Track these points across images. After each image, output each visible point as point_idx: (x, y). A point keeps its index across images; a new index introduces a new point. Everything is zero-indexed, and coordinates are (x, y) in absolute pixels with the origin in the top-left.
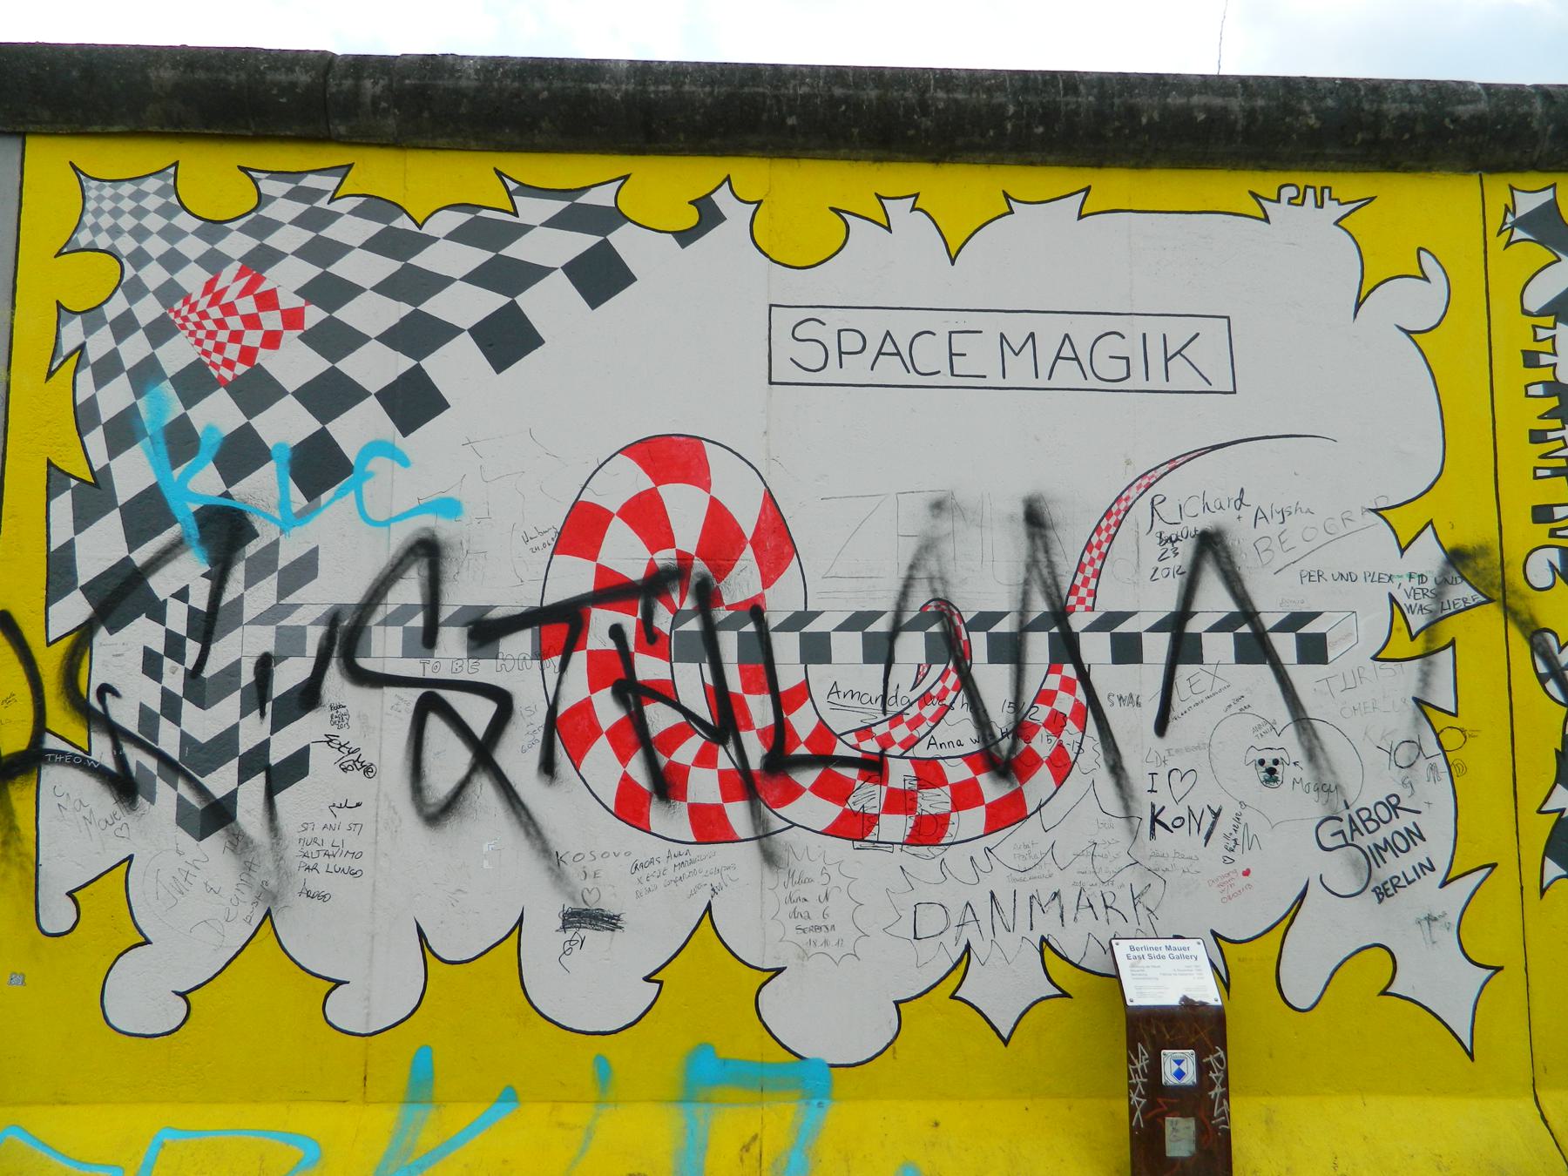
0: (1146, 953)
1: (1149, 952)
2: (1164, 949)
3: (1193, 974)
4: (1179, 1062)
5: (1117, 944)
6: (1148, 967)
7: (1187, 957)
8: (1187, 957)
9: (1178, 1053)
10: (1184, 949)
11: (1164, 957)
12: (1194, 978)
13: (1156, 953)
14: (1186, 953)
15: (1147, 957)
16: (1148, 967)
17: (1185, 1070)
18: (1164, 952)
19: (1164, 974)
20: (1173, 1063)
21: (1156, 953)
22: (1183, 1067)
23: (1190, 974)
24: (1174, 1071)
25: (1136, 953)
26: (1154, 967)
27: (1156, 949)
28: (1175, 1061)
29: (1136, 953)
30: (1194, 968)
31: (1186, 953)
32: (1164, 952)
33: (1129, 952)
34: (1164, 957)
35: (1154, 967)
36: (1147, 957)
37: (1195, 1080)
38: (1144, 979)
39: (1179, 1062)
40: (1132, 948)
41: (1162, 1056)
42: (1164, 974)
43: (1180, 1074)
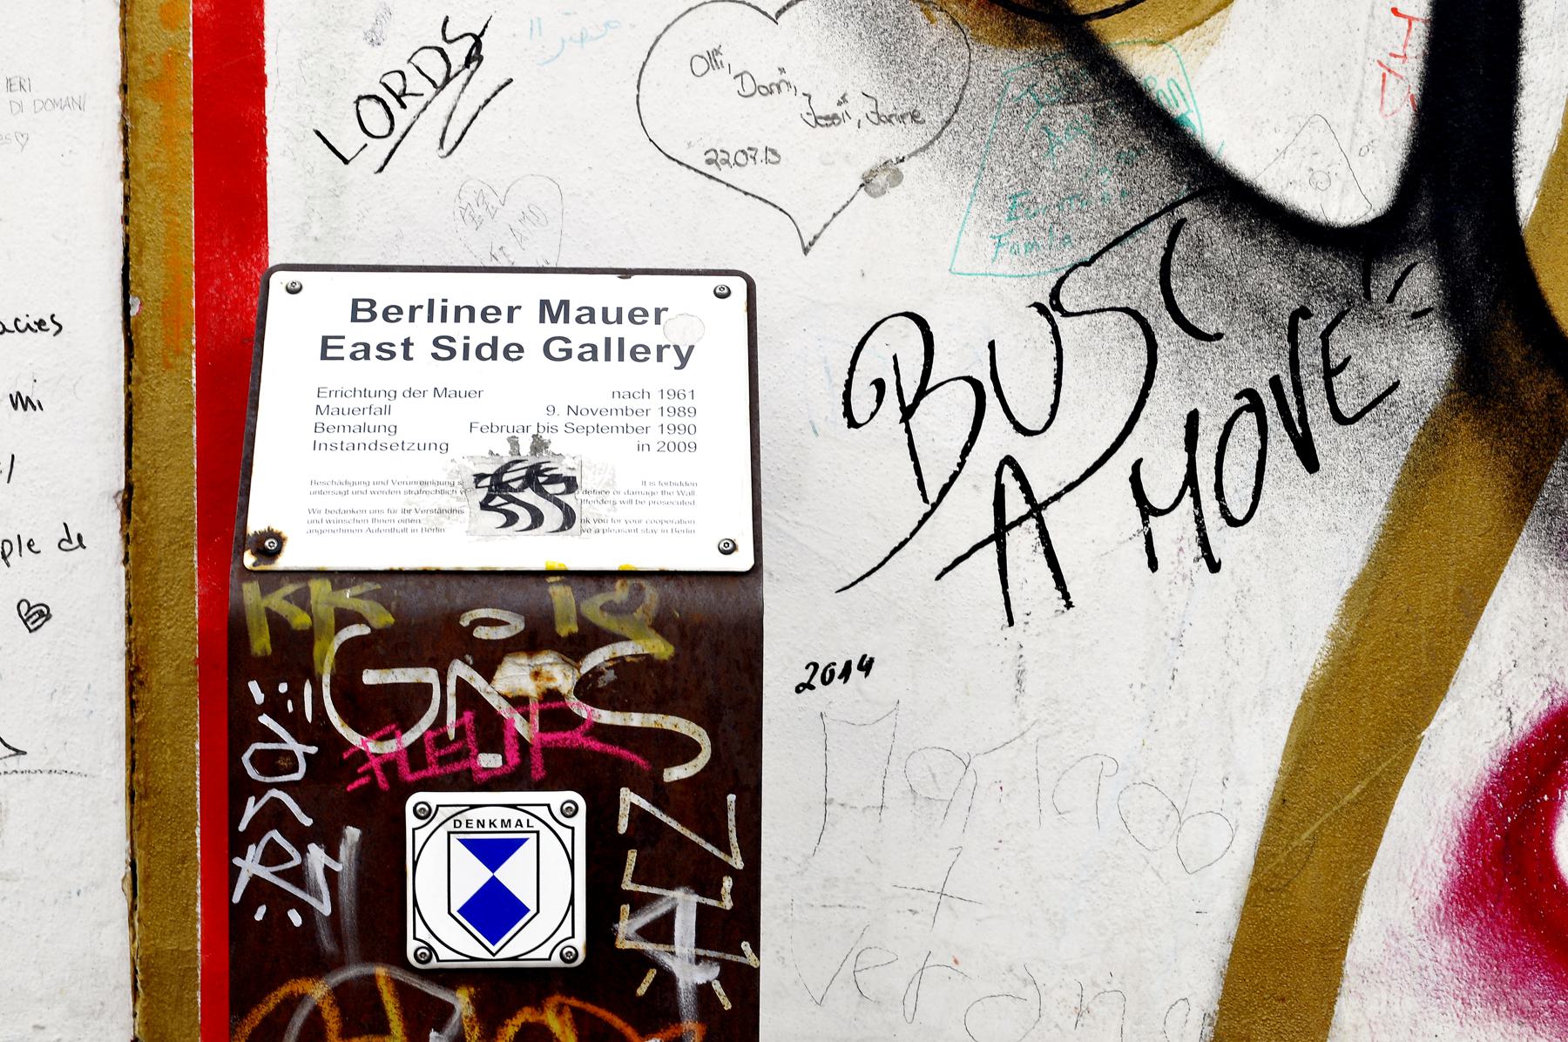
0: (423, 333)
1: (450, 328)
4: (493, 852)
8: (638, 353)
11: (514, 352)
12: (640, 448)
13: (480, 332)
14: (633, 335)
15: (422, 349)
17: (526, 896)
18: (529, 331)
20: (462, 855)
21: (480, 332)
22: (515, 875)
23: (625, 429)
24: (461, 898)
25: (376, 332)
27: (488, 314)
28: (473, 846)
29: (376, 332)
30: (655, 403)
31: (633, 335)
33: (338, 322)
34: (514, 352)
36: (422, 349)
37: (579, 942)
39: (493, 852)
40: (361, 310)
41: (411, 821)
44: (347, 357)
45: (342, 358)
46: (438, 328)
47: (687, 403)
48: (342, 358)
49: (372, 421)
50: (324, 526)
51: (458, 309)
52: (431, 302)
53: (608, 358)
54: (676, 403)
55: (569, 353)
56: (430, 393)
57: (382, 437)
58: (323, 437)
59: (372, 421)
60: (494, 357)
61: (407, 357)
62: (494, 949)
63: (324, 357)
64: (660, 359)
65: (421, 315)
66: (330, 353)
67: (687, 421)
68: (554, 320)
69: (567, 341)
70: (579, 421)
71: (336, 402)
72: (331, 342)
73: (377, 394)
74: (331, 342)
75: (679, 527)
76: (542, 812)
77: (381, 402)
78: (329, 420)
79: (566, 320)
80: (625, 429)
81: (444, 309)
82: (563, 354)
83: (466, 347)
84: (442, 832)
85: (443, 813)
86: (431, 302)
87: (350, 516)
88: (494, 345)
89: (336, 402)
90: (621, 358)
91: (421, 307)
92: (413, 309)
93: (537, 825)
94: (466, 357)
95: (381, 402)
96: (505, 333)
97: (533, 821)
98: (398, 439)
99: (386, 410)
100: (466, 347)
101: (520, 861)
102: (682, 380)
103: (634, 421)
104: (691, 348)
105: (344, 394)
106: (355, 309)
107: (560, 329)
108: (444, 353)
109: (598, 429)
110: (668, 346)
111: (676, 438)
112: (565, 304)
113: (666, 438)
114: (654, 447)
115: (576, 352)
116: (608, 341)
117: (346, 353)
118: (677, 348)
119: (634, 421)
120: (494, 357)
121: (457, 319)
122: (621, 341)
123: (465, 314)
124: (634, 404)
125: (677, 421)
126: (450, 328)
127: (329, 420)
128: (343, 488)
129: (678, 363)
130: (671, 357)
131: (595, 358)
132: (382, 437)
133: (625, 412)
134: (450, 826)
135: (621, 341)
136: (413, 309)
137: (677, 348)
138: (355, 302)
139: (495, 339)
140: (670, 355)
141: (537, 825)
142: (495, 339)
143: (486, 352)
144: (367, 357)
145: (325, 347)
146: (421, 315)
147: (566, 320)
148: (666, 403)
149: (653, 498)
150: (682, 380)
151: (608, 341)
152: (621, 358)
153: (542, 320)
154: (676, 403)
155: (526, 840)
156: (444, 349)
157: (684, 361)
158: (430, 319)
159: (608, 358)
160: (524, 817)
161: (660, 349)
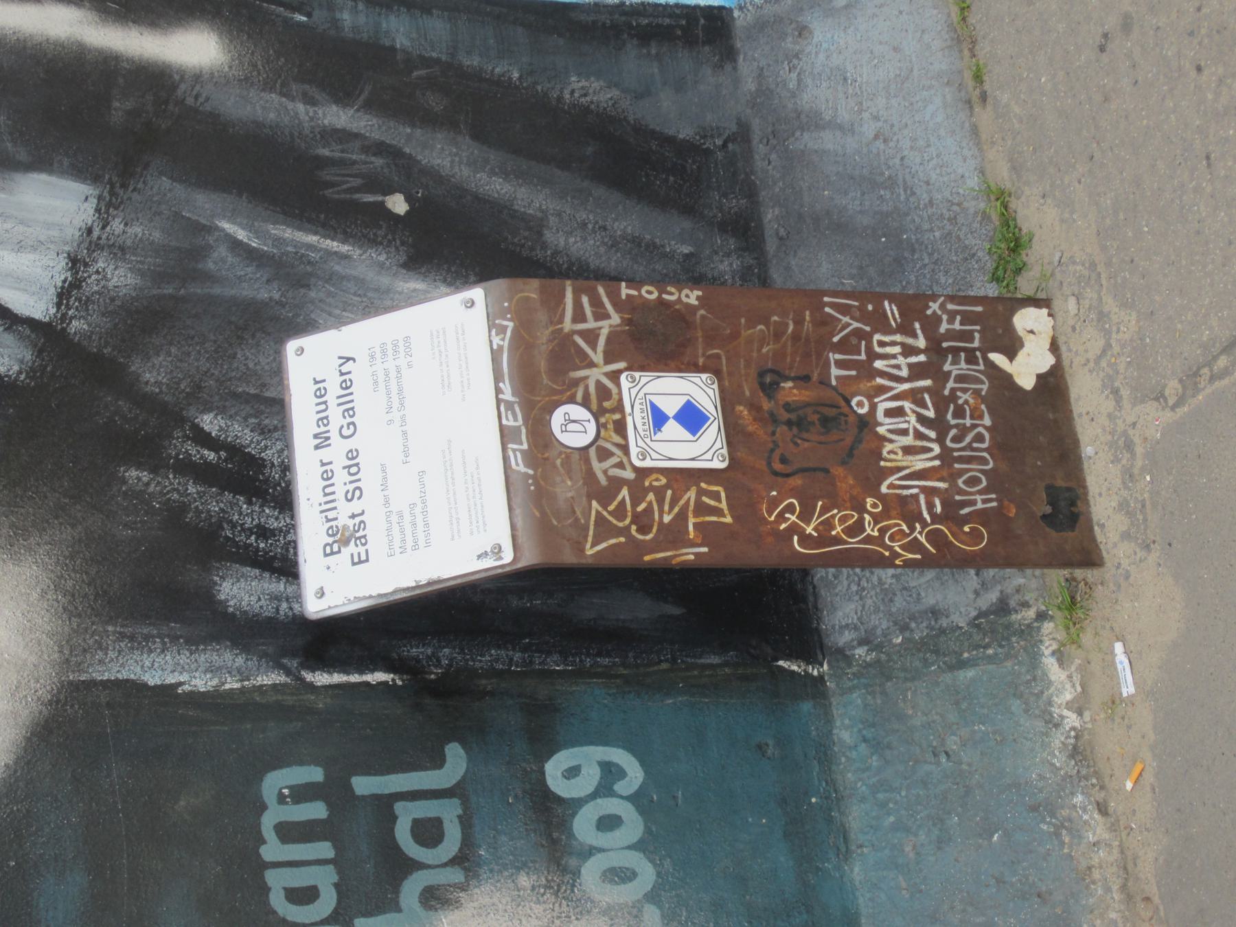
1: (340, 496)
2: (324, 454)
3: (398, 368)
4: (659, 418)
5: (321, 593)
6: (387, 502)
7: (346, 386)
8: (346, 386)
9: (637, 420)
10: (320, 394)
11: (352, 455)
12: (410, 366)
13: (341, 477)
14: (334, 390)
16: (387, 502)
18: (336, 452)
19: (406, 453)
21: (341, 477)
22: (671, 407)
23: (399, 378)
26: (384, 487)
27: (327, 477)
32: (336, 452)
34: (352, 455)
35: (384, 487)
36: (356, 506)
38: (425, 512)
42: (406, 453)
43: (691, 418)
44: (366, 547)
45: (367, 551)
46: (341, 503)
47: (378, 350)
48: (367, 551)
49: (407, 518)
50: (481, 522)
51: (326, 495)
52: (322, 512)
53: (352, 401)
54: (378, 355)
55: (349, 424)
56: (386, 493)
57: (418, 510)
58: (421, 543)
59: (407, 518)
60: (357, 465)
61: (363, 513)
62: (712, 418)
63: (367, 560)
64: (350, 373)
65: (331, 515)
66: (363, 557)
67: (389, 347)
68: (328, 438)
69: (342, 427)
70: (396, 404)
71: (397, 543)
72: (356, 560)
73: (389, 522)
74: (356, 560)
75: (460, 332)
76: (634, 392)
77: (394, 518)
78: (410, 543)
79: (328, 431)
80: (399, 378)
81: (326, 503)
82: (351, 426)
83: (351, 482)
84: (652, 444)
85: (641, 443)
86: (322, 512)
87: (473, 512)
88: (349, 467)
89: (397, 543)
90: (351, 394)
91: (326, 517)
92: (328, 520)
93: (641, 395)
94: (359, 480)
95: (394, 518)
96: (340, 461)
97: (639, 396)
98: (419, 502)
99: (401, 516)
100: (351, 482)
101: (662, 404)
102: (363, 359)
103: (393, 374)
104: (340, 358)
105: (391, 541)
106: (332, 553)
107: (334, 434)
108: (357, 493)
109: (400, 391)
110: (340, 371)
111: (402, 349)
112: (316, 436)
113: (402, 354)
114: (409, 359)
115: (349, 420)
116: (339, 405)
117: (362, 550)
118: (340, 366)
119: (393, 374)
120: (357, 465)
121: (333, 493)
122: (339, 397)
123: (328, 490)
124: (381, 378)
125: (390, 352)
126: (340, 496)
127: (410, 543)
128: (454, 521)
129: (351, 362)
131: (352, 409)
132: (418, 510)
133: (387, 381)
134: (648, 440)
135: (339, 397)
136: (328, 520)
137: (340, 366)
138: (326, 555)
139: (344, 468)
140: (344, 369)
141: (641, 395)
142: (344, 468)
143: (354, 470)
144: (364, 537)
145: (360, 562)
146: (331, 515)
147: (328, 431)
148: (379, 361)
149: (443, 350)
150: (363, 359)
151: (339, 405)
153: (329, 445)
154: (378, 355)
155: (651, 402)
156: (354, 494)
157: (348, 359)
158: (335, 508)
160: (637, 402)
161: (342, 374)
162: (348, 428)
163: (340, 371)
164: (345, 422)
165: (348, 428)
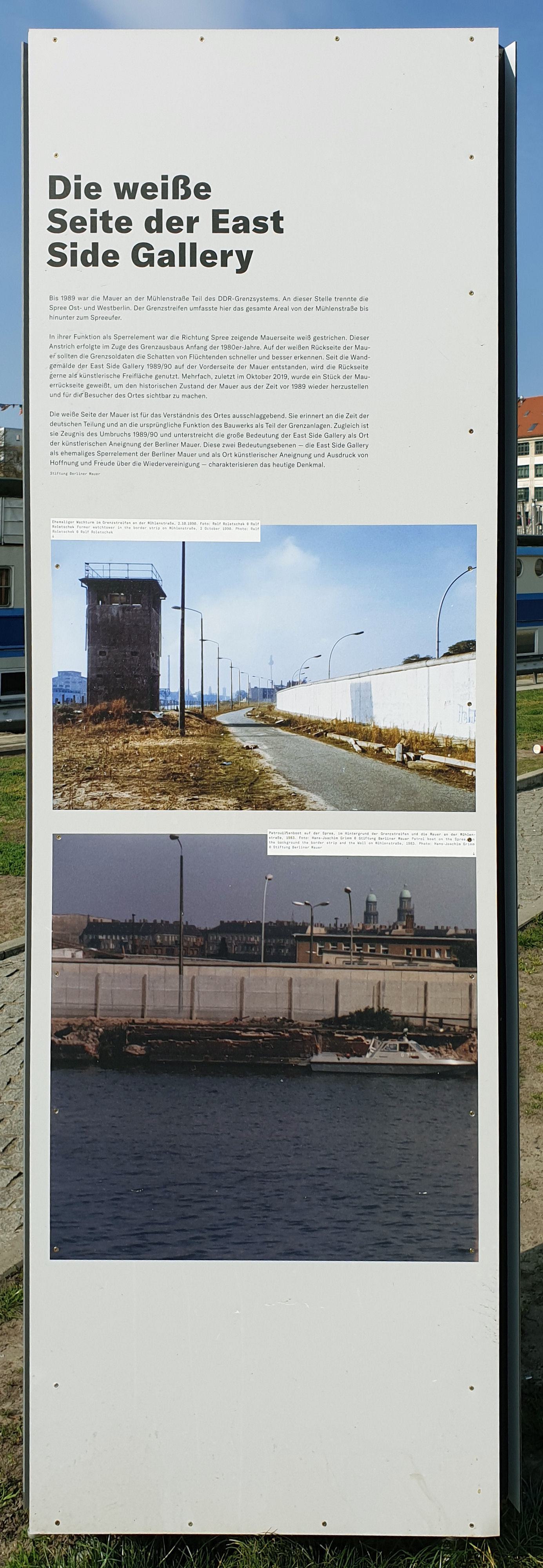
53: (182, 264)
55: (151, 257)
69: (150, 247)
82: (146, 260)
83: (74, 253)
90: (193, 264)
104: (250, 253)
110: (231, 253)
115: (157, 258)
118: (239, 253)
120: (95, 263)
122: (193, 246)
129: (239, 267)
130: (234, 262)
131: (172, 264)
137: (239, 253)
143: (90, 258)
152: (193, 264)
159: (182, 264)
162: (145, 255)
163: (231, 253)
164: (156, 252)
165: (145, 255)
